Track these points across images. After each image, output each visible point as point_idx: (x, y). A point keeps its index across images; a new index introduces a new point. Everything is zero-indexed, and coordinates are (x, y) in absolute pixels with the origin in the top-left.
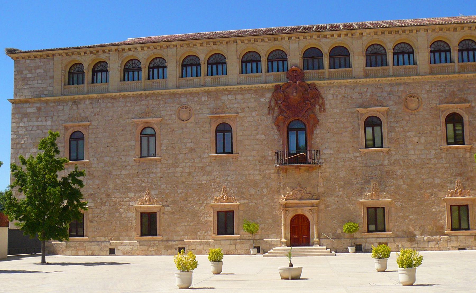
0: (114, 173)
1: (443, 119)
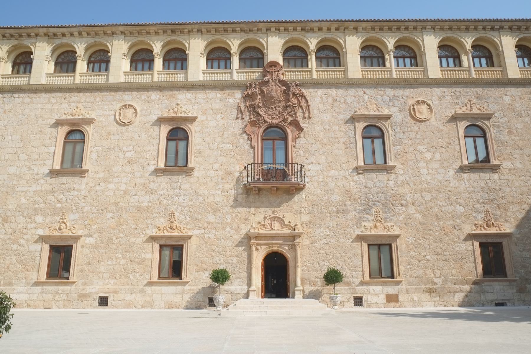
0: (20, 189)
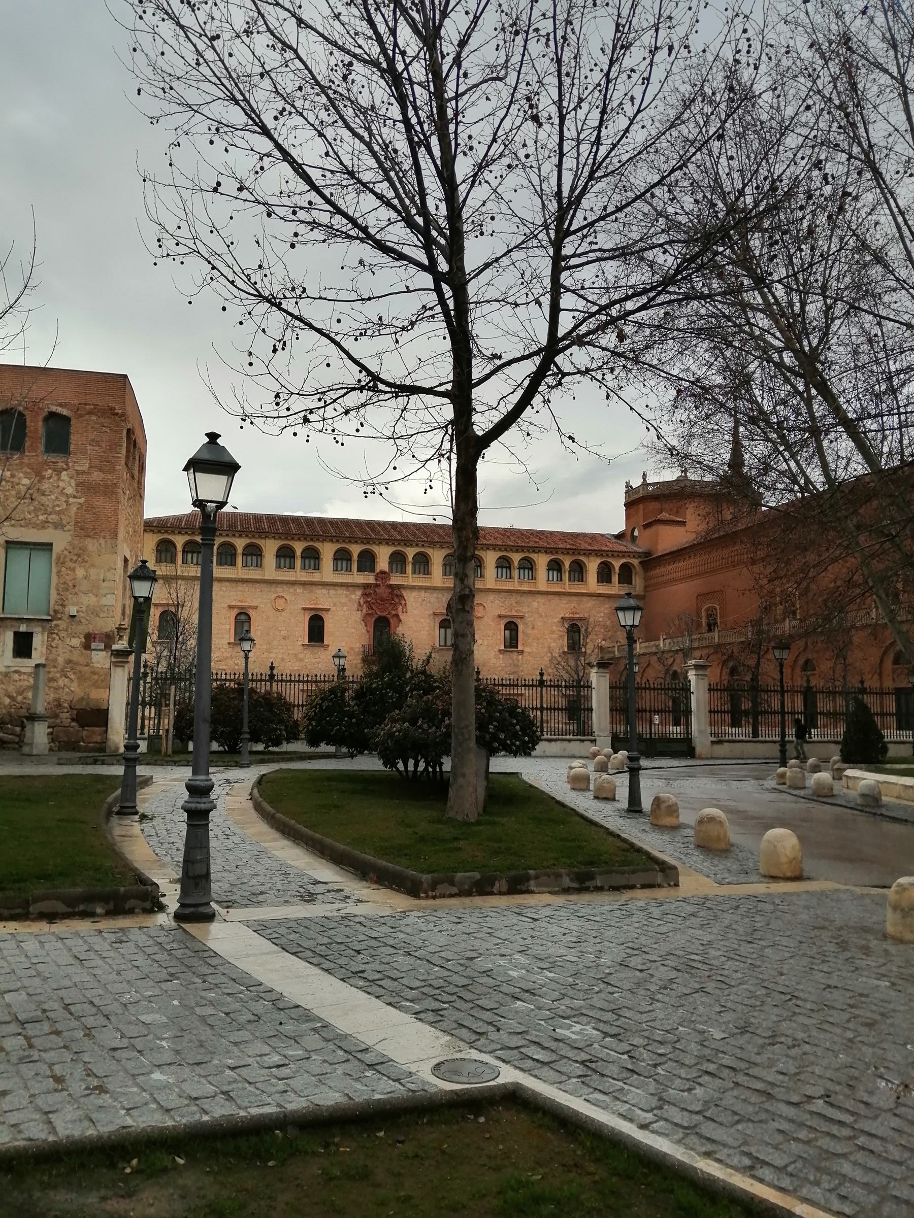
1: (503, 627)
